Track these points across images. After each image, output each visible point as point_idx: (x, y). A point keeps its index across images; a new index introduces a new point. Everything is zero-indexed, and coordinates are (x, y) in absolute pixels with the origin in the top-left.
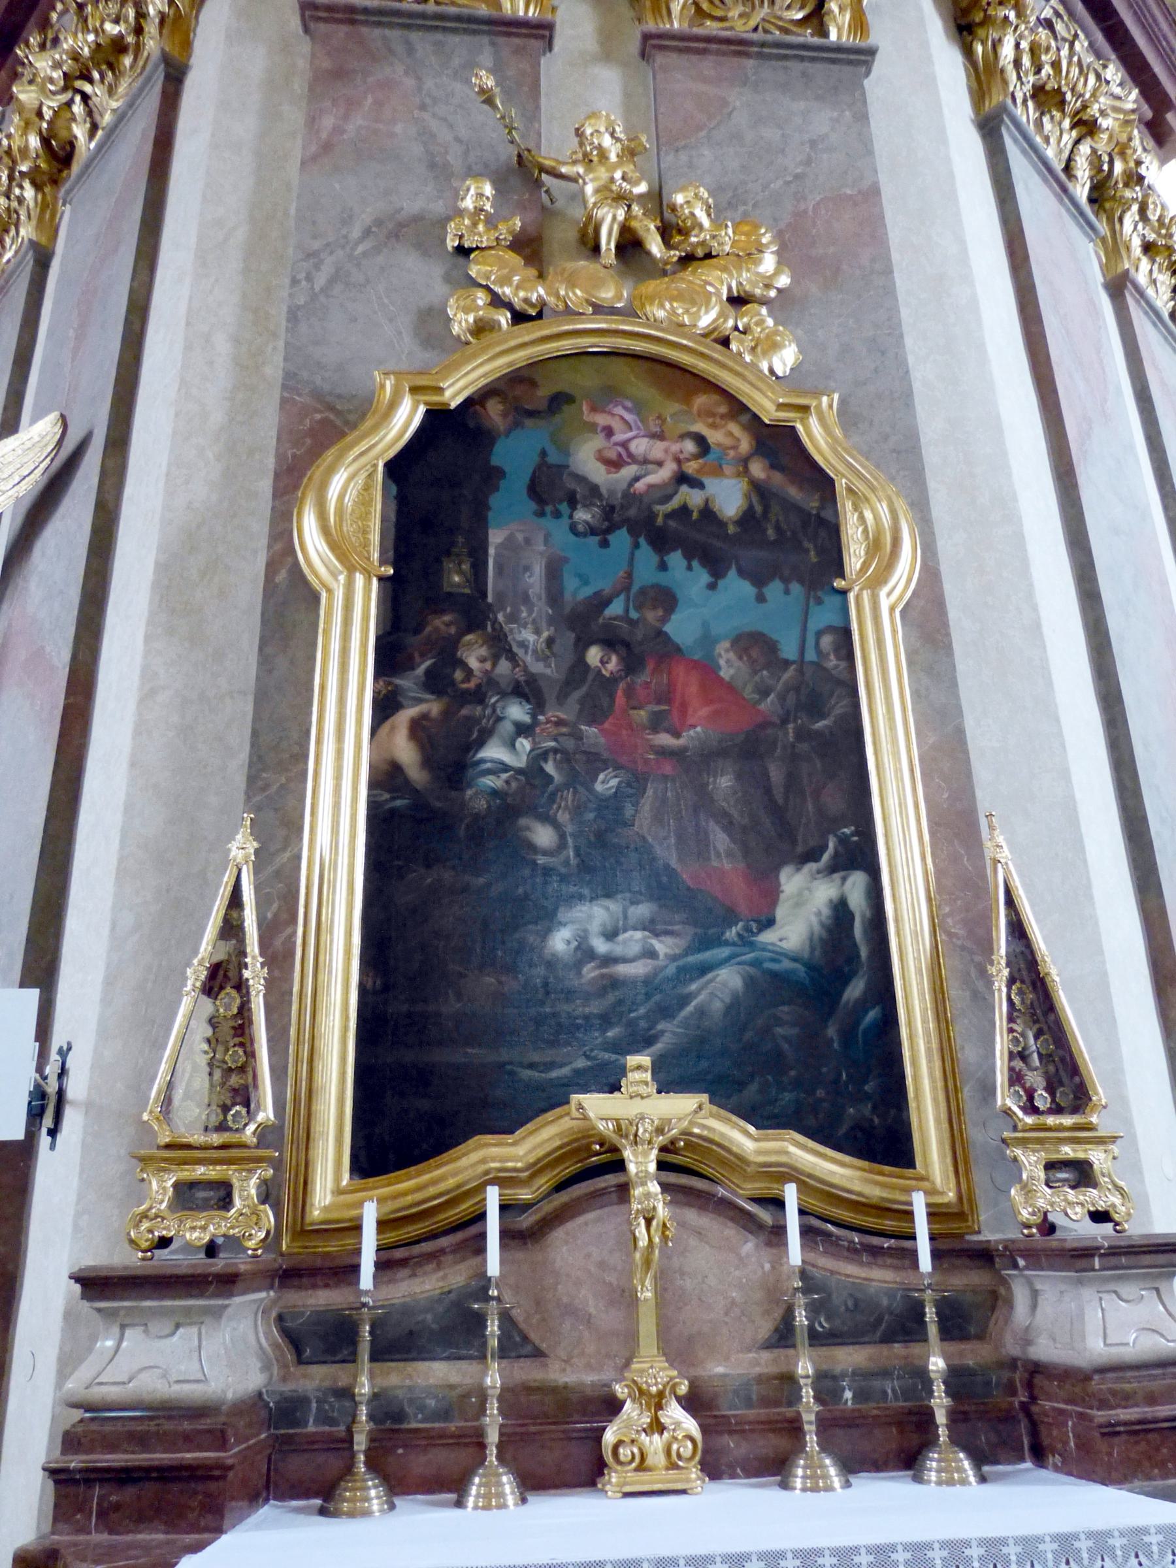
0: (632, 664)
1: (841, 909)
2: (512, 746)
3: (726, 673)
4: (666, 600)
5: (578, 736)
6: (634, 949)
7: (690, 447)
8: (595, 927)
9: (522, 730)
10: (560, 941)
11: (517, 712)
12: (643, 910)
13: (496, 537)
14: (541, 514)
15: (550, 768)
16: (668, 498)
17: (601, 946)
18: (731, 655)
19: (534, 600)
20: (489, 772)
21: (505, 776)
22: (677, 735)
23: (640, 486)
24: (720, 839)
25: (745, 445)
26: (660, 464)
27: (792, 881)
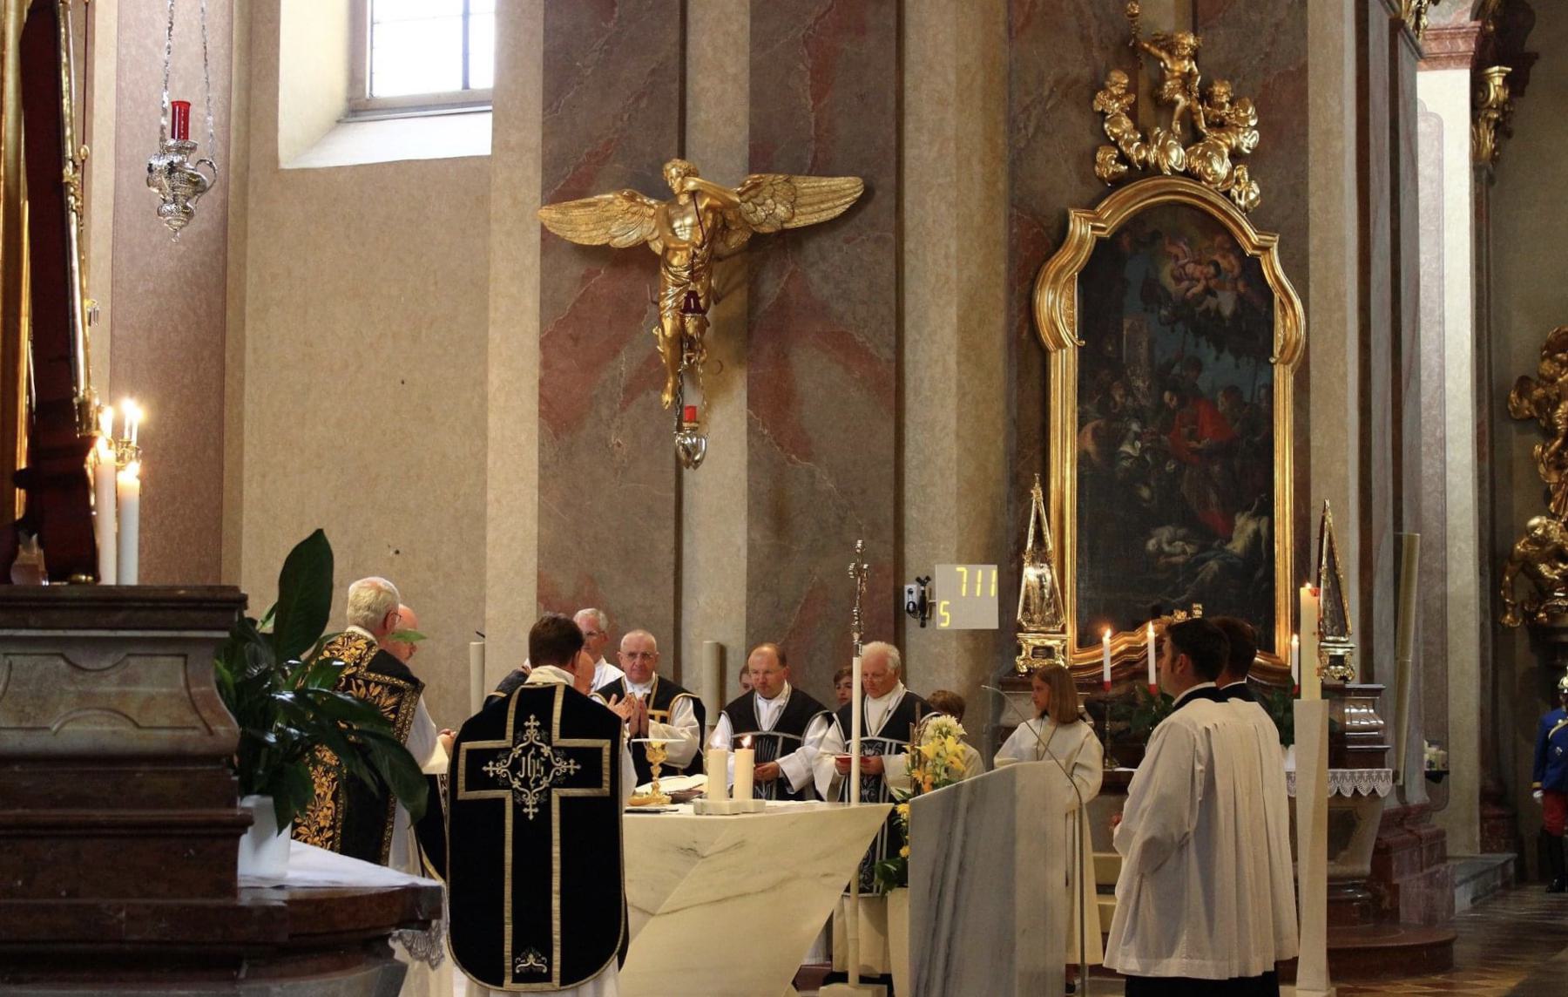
0: (1183, 402)
1: (1257, 533)
2: (1133, 445)
3: (1220, 409)
4: (1198, 365)
5: (1159, 441)
6: (1178, 550)
7: (1212, 270)
8: (1164, 539)
9: (1138, 436)
10: (1151, 545)
11: (1135, 427)
12: (1182, 532)
13: (1127, 324)
14: (1146, 310)
15: (1148, 457)
16: (1200, 303)
17: (1166, 548)
18: (1224, 399)
19: (1142, 362)
20: (1123, 458)
21: (1130, 460)
22: (1199, 442)
23: (1189, 294)
24: (1213, 498)
25: (1237, 271)
26: (1198, 280)
27: (1240, 520)
